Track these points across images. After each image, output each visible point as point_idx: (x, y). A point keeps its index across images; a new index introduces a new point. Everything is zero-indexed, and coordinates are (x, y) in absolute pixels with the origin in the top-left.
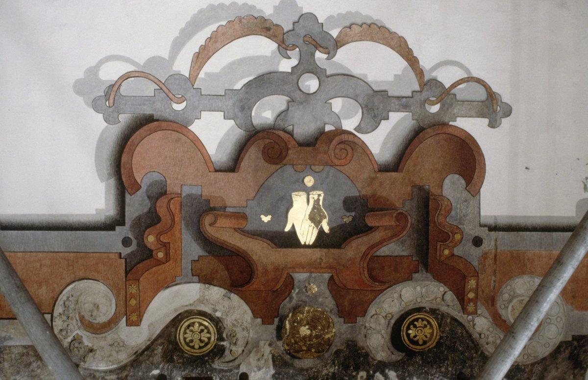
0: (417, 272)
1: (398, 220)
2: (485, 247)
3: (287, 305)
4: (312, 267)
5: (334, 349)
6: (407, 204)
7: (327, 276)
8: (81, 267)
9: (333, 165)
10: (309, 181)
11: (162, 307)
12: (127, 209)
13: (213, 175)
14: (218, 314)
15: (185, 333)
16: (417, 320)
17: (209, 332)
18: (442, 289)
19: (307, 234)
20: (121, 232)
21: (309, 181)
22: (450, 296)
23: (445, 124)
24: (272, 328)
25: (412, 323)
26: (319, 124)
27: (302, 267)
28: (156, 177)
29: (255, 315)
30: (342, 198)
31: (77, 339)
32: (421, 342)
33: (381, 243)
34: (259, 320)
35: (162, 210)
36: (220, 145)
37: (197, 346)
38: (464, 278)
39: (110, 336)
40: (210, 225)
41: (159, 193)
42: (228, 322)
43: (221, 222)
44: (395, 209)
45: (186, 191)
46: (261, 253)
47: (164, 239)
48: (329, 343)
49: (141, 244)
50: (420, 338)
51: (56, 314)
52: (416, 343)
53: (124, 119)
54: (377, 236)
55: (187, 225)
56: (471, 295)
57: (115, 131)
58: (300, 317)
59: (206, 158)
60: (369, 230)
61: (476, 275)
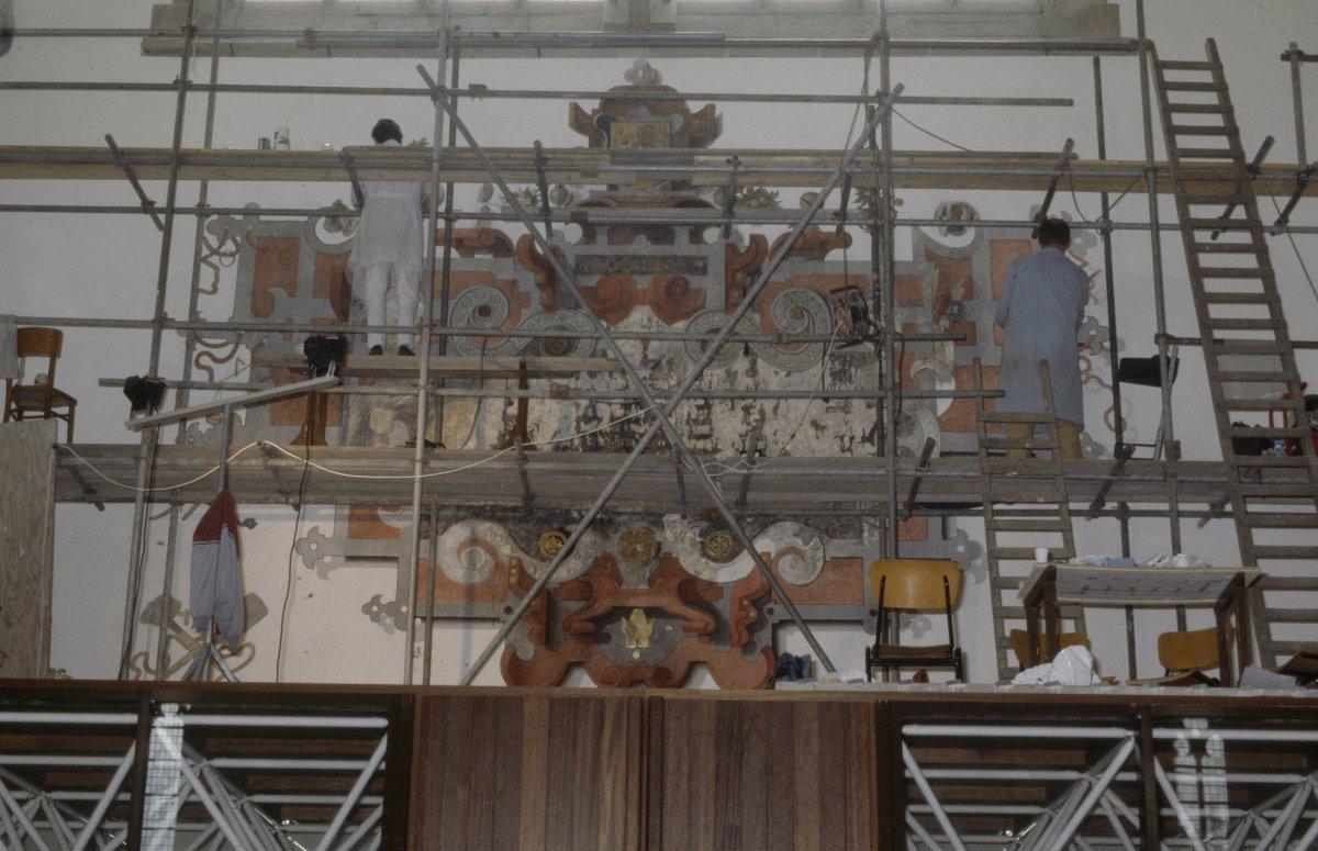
1: (570, 627)
3: (654, 566)
4: (635, 594)
5: (618, 535)
7: (624, 587)
10: (636, 655)
11: (743, 566)
12: (770, 635)
13: (707, 659)
14: (703, 560)
19: (638, 618)
20: (774, 619)
21: (636, 655)
24: (665, 549)
27: (642, 593)
28: (750, 658)
29: (677, 561)
31: (806, 543)
33: (579, 612)
34: (674, 555)
35: (745, 637)
39: (782, 545)
40: (708, 624)
41: (748, 647)
42: (696, 555)
43: (702, 625)
45: (727, 648)
46: (671, 603)
47: (743, 614)
49: (760, 610)
50: (554, 540)
51: (821, 562)
52: (557, 537)
55: (727, 624)
56: (514, 571)
58: (645, 558)
60: (594, 620)
61: (510, 586)
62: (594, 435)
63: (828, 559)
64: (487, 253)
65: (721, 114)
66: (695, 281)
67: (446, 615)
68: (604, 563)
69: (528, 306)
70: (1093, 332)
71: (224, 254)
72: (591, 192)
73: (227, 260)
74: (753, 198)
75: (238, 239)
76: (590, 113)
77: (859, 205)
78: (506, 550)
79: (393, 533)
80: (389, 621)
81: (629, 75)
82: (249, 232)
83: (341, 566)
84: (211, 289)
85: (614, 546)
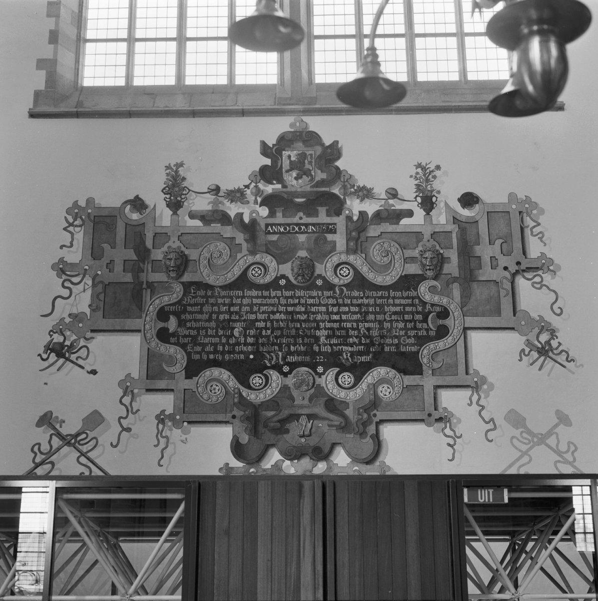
0: (259, 405)
2: (231, 415)
6: (263, 432)
8: (394, 406)
9: (294, 447)
15: (351, 381)
16: (259, 386)
17: (342, 381)
18: (249, 398)
20: (377, 419)
22: (244, 394)
23: (247, 464)
25: (261, 385)
26: (300, 462)
28: (364, 441)
30: (290, 433)
32: (257, 377)
36: (339, 453)
37: (346, 376)
38: (239, 402)
44: (268, 430)
45: (352, 436)
48: (294, 377)
49: (369, 415)
53: (377, 463)
54: (276, 419)
55: (351, 422)
57: (381, 458)
59: (344, 448)
60: (279, 421)
61: (234, 404)
62: (278, 321)
63: (405, 386)
64: (218, 224)
65: (342, 145)
66: (330, 237)
67: (201, 420)
68: (285, 389)
69: (241, 251)
70: (543, 261)
71: (76, 226)
72: (273, 189)
73: (78, 229)
74: (360, 191)
75: (84, 217)
76: (272, 147)
77: (417, 194)
78: (233, 383)
79: (172, 376)
80: (170, 424)
81: (291, 125)
82: (89, 214)
83: (144, 394)
84: (69, 245)
85: (290, 381)
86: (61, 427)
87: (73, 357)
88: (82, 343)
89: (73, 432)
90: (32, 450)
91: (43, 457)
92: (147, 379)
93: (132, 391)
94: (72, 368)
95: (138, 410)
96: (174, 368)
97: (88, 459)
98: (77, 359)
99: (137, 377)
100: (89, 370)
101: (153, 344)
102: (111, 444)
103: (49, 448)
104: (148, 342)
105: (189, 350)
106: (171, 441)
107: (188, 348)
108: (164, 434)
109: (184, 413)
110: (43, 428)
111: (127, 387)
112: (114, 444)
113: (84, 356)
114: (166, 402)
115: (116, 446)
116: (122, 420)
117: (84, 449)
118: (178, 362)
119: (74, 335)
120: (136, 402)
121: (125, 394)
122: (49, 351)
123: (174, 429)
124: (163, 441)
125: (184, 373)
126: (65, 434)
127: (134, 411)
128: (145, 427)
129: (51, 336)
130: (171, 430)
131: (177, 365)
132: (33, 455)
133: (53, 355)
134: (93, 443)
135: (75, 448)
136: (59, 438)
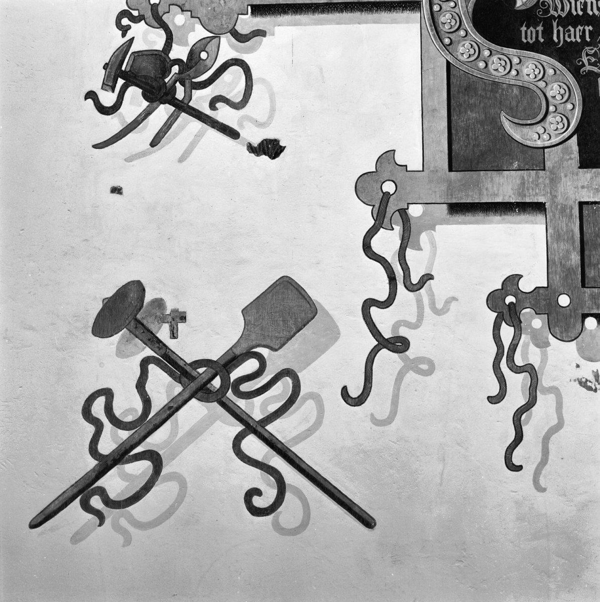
79: (533, 159)
80: (538, 323)
86: (174, 335)
87: (200, 99)
88: (227, 49)
89: (215, 353)
90: (87, 413)
91: (124, 435)
92: (450, 170)
93: (403, 212)
94: (199, 136)
95: (427, 277)
96: (539, 129)
97: (271, 442)
98: (212, 106)
99: (415, 164)
100: (256, 142)
101: (464, 50)
102: (345, 392)
103: (139, 406)
104: (447, 41)
105: (588, 68)
106: (545, 381)
107: (585, 59)
108: (519, 361)
109: (583, 286)
110: (116, 338)
111: (387, 195)
112: (354, 392)
113: (236, 94)
114: (522, 249)
115: (359, 401)
116: (374, 311)
117: (256, 409)
118: (552, 108)
119: (198, 27)
120: (420, 249)
121: (380, 221)
122: (121, 82)
123: (552, 339)
124: (516, 382)
125: (575, 148)
126: (189, 360)
127: (415, 279)
128: (457, 338)
129: (125, 30)
130: (543, 345)
131: (550, 118)
132: (91, 429)
133: (134, 93)
134: (283, 388)
135: (223, 405)
136: (171, 374)
